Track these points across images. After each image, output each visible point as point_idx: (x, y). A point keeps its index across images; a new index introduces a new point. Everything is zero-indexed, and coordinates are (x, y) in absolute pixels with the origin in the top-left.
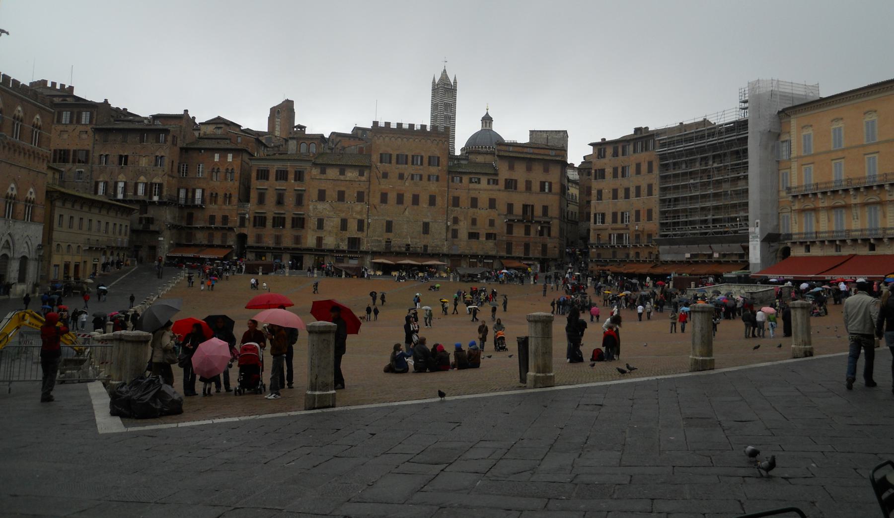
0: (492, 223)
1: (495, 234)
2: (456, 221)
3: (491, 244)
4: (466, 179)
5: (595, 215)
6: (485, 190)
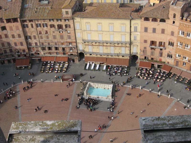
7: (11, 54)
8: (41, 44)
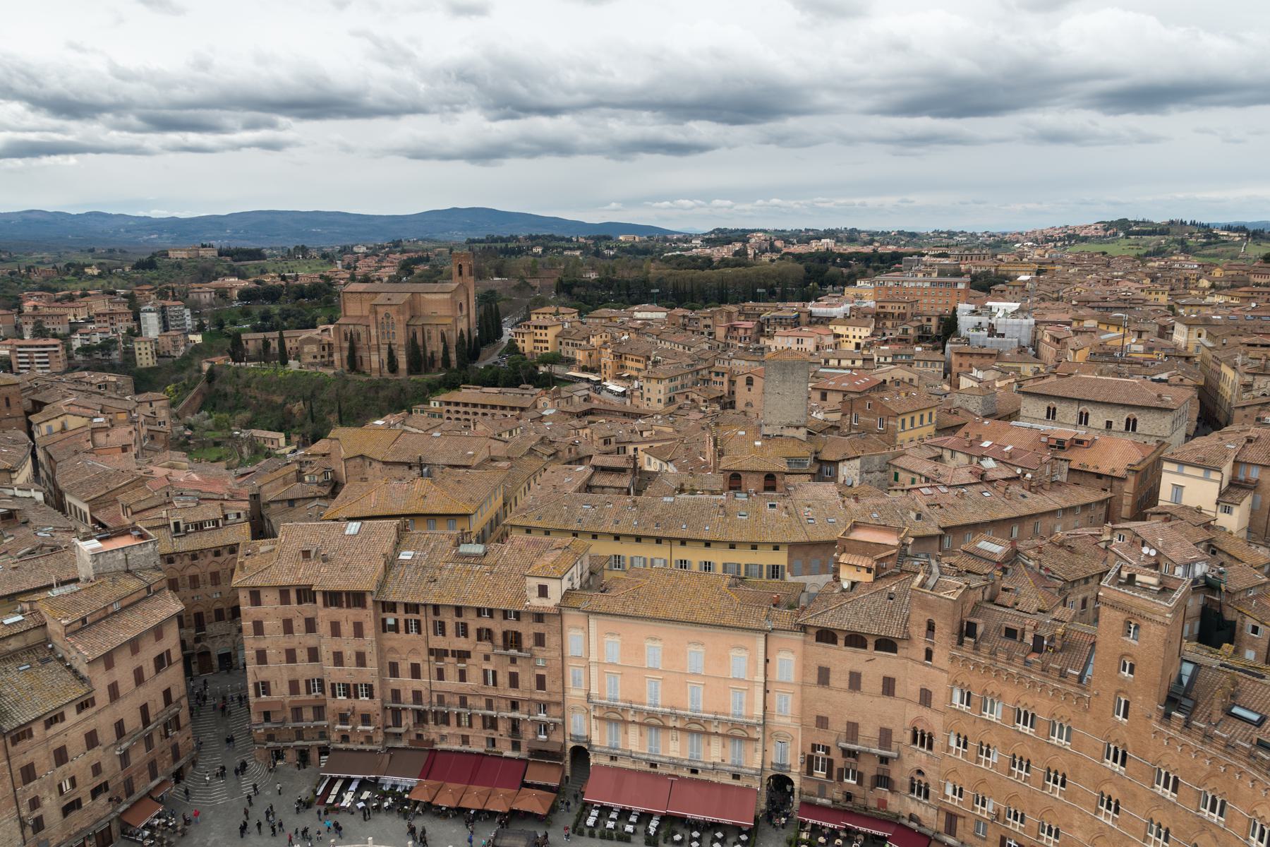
0: (97, 769)
1: (106, 783)
2: (35, 803)
3: (103, 799)
4: (38, 730)
5: (256, 685)
6: (75, 725)
7: (316, 727)
8: (435, 699)
